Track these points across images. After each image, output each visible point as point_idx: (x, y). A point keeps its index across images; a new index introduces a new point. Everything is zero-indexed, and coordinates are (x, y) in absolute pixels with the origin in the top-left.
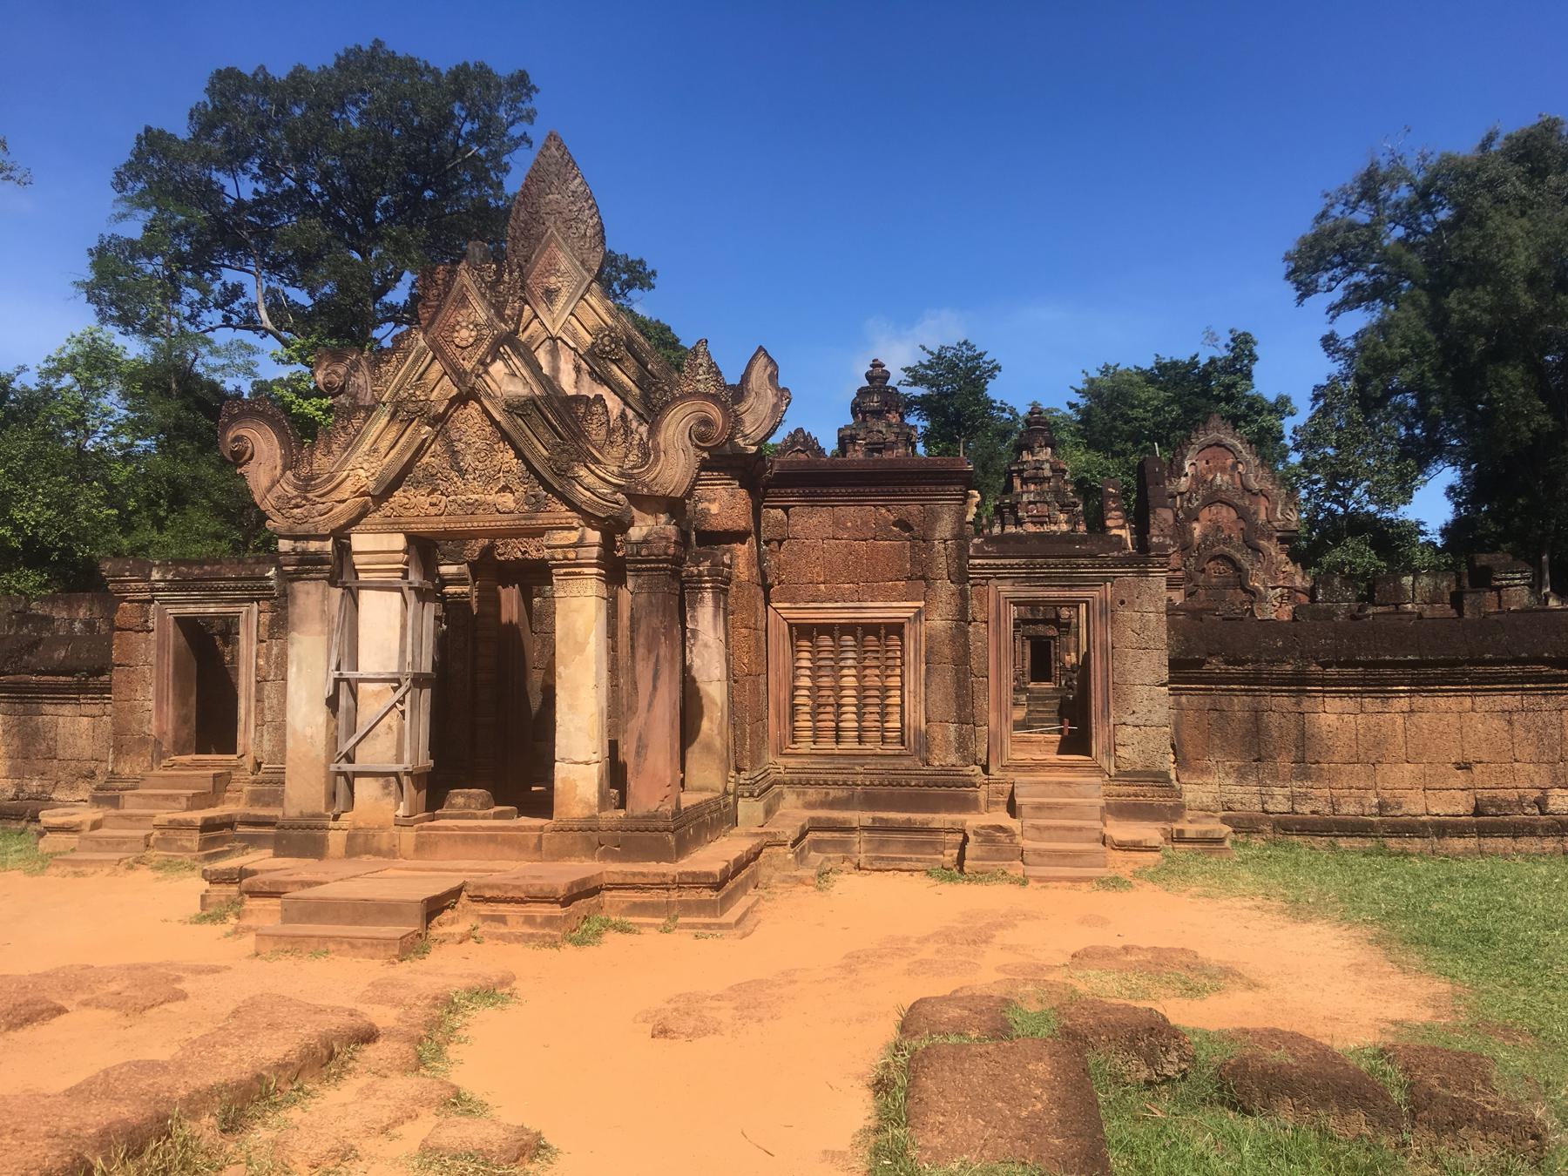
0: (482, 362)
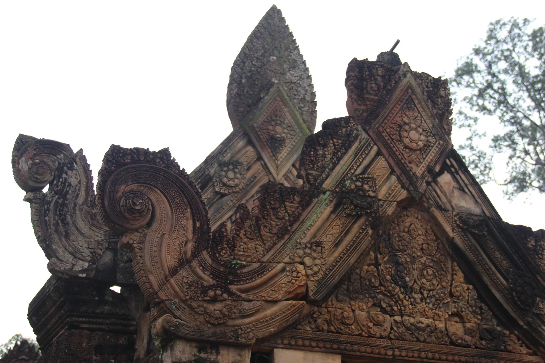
0: (430, 170)
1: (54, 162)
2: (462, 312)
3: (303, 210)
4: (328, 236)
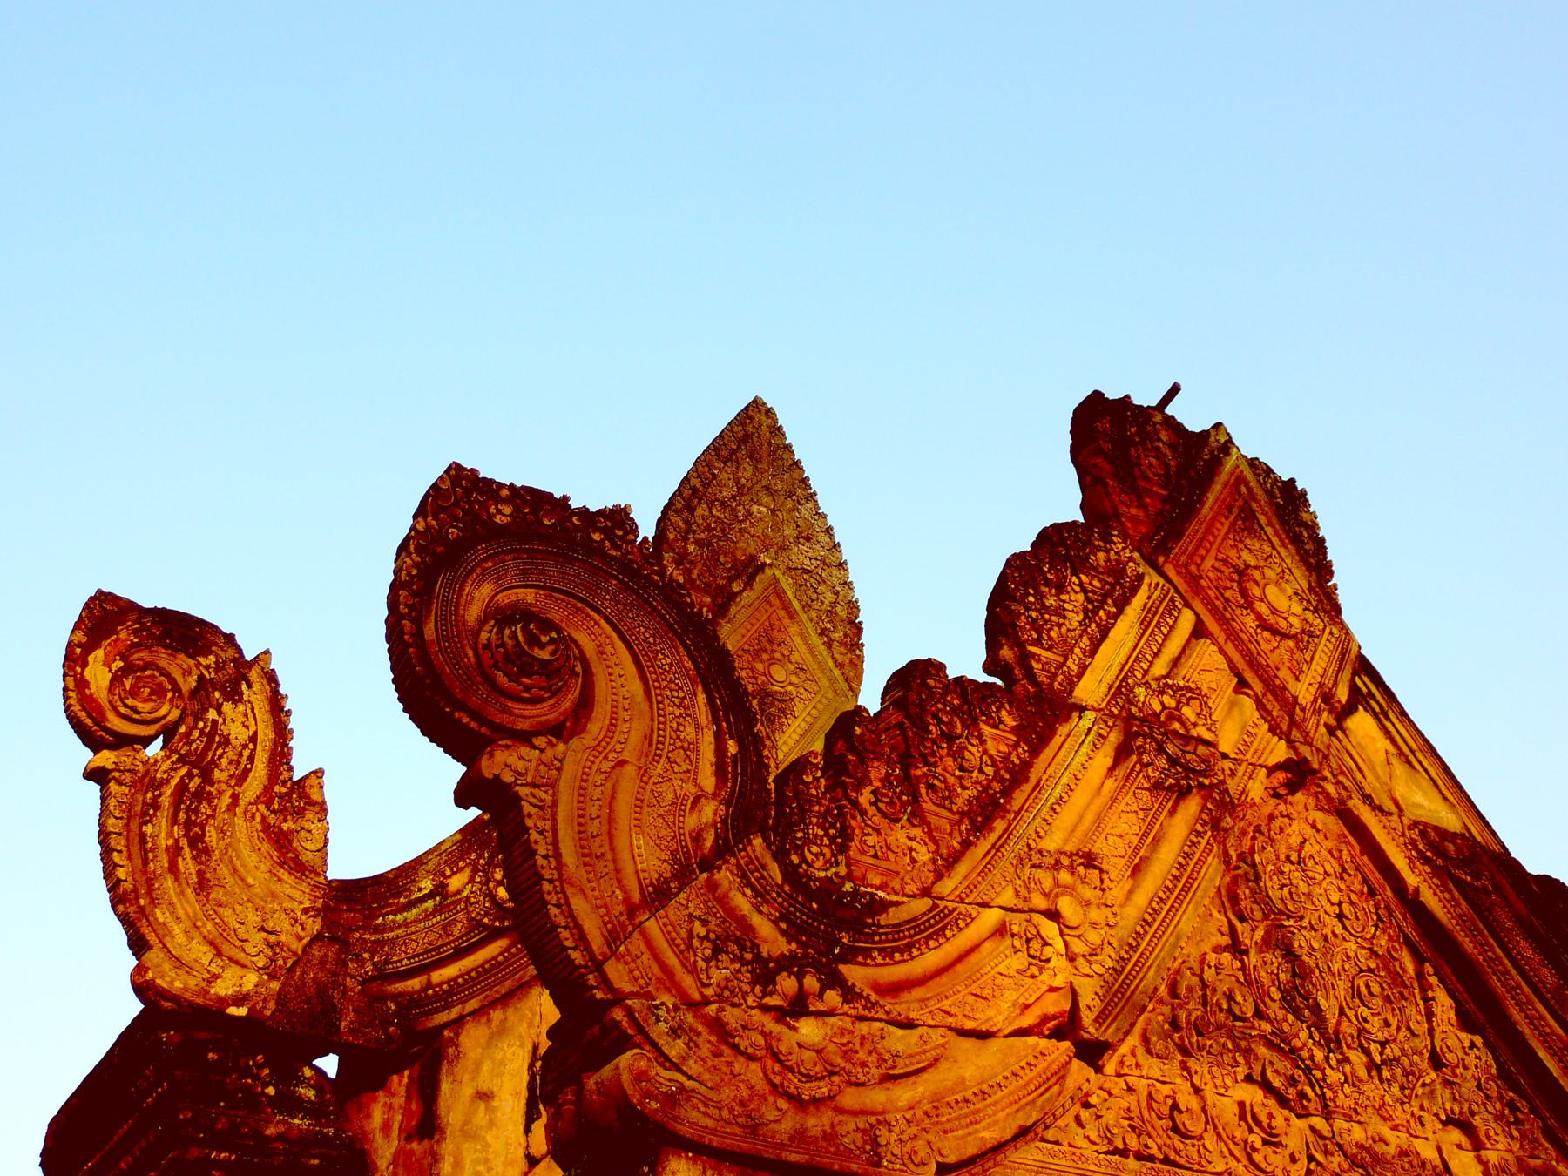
1: (187, 672)
2: (1473, 1114)
3: (1035, 751)
4: (1111, 838)
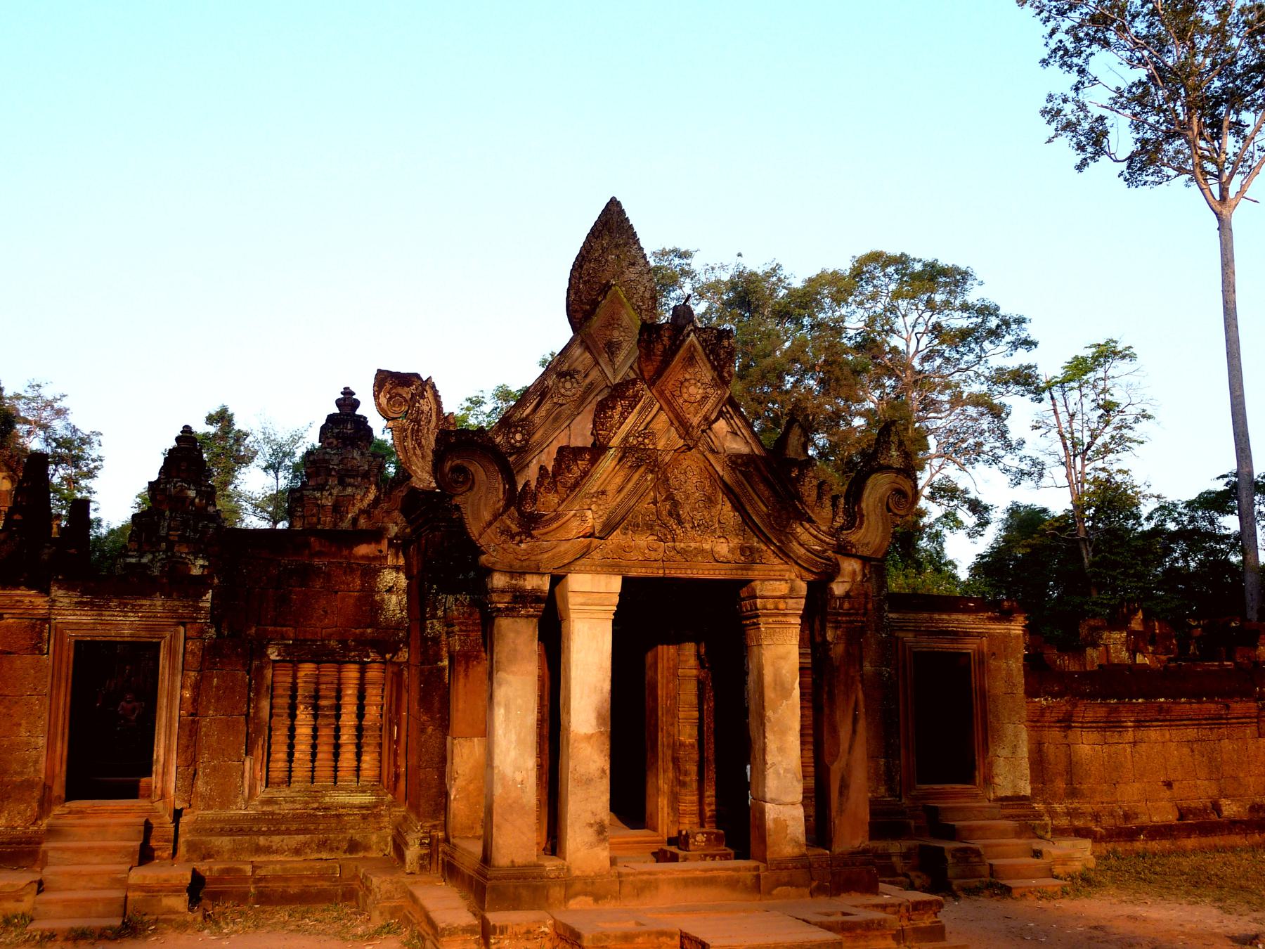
0: (706, 418)
